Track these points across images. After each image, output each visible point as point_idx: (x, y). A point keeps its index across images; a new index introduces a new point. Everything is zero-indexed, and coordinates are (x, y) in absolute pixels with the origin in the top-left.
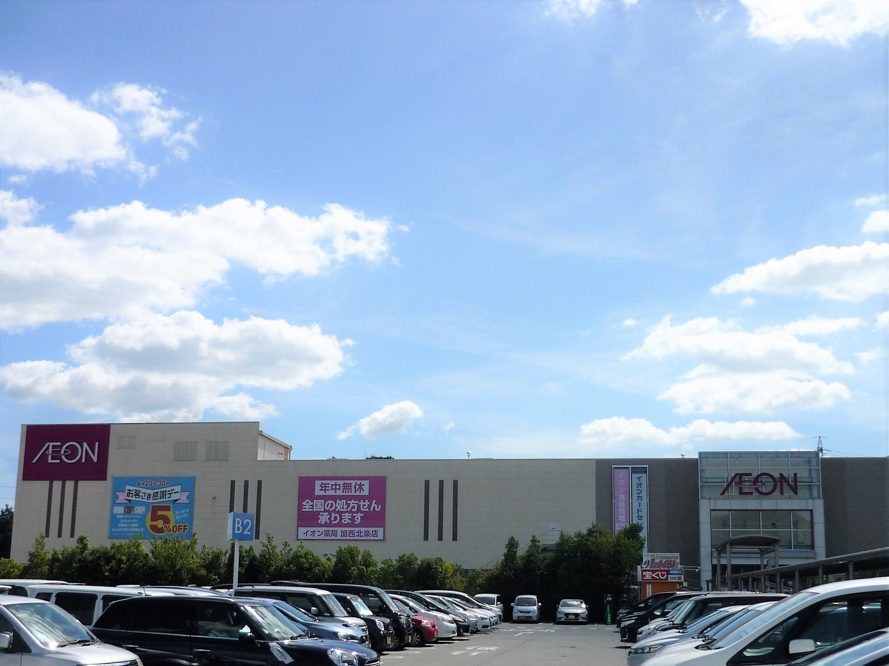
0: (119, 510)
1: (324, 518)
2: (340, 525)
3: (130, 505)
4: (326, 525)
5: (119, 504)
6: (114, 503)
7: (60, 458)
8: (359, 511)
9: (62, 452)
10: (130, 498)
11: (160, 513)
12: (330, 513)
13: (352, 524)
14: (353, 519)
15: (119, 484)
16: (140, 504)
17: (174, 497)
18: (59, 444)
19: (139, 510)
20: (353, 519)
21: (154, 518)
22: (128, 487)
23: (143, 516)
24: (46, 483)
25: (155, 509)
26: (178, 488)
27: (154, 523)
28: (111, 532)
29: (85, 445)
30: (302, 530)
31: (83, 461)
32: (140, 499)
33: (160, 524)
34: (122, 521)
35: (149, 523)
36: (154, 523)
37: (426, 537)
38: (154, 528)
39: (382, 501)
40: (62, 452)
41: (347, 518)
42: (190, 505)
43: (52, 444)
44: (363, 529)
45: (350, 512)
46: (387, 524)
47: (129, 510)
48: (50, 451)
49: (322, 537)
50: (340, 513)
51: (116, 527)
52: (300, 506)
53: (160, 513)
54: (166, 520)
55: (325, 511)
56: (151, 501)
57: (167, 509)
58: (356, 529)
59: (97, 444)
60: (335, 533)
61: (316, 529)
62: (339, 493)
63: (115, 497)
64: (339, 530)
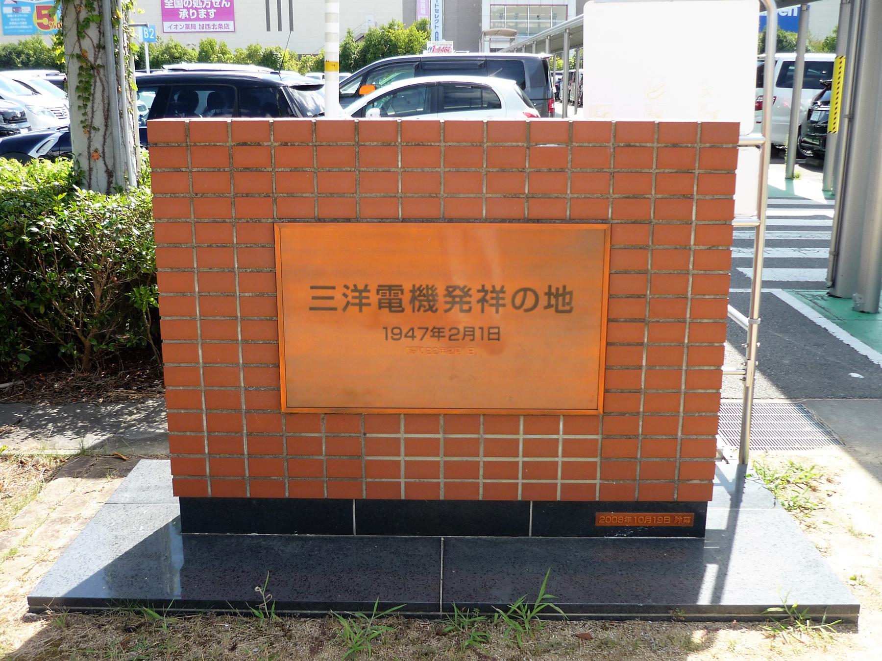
1: (183, 14)
2: (198, 19)
3: (16, 6)
4: (186, 19)
12: (188, 9)
13: (208, 18)
14: (207, 14)
19: (26, 10)
20: (207, 14)
21: (40, 16)
27: (40, 21)
28: (4, 30)
30: (167, 24)
35: (36, 21)
36: (40, 21)
37: (268, 29)
38: (41, 25)
41: (202, 14)
44: (217, 23)
45: (205, 8)
49: (184, 30)
50: (196, 9)
51: (8, 25)
55: (184, 7)
58: (211, 23)
60: (194, 27)
61: (178, 23)
64: (197, 23)
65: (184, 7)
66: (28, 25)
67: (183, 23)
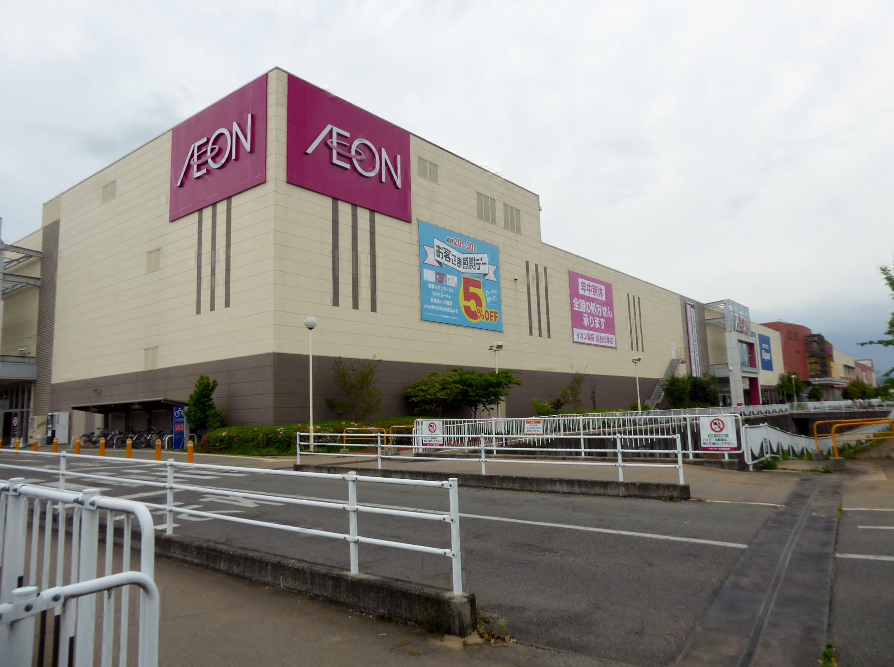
0: (430, 275)
3: (440, 270)
4: (588, 328)
5: (430, 267)
6: (423, 265)
7: (350, 161)
8: (602, 317)
9: (353, 152)
10: (439, 259)
11: (472, 290)
15: (427, 234)
16: (454, 272)
17: (484, 269)
18: (347, 134)
19: (452, 281)
21: (468, 296)
22: (437, 242)
23: (456, 289)
24: (328, 202)
25: (468, 283)
26: (485, 258)
27: (467, 304)
28: (422, 310)
29: (384, 155)
30: (576, 331)
31: (384, 180)
32: (450, 264)
33: (472, 304)
34: (434, 294)
36: (467, 304)
38: (467, 309)
39: (612, 310)
40: (353, 152)
42: (496, 284)
43: (336, 130)
46: (617, 331)
47: (441, 279)
48: (335, 140)
49: (586, 341)
50: (594, 316)
52: (572, 305)
53: (472, 290)
54: (479, 303)
56: (461, 269)
57: (477, 284)
59: (399, 157)
62: (591, 295)
63: (423, 255)
65: (586, 312)
66: (453, 307)
67: (586, 332)
